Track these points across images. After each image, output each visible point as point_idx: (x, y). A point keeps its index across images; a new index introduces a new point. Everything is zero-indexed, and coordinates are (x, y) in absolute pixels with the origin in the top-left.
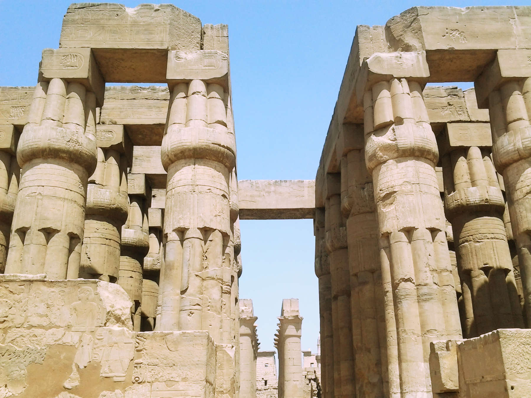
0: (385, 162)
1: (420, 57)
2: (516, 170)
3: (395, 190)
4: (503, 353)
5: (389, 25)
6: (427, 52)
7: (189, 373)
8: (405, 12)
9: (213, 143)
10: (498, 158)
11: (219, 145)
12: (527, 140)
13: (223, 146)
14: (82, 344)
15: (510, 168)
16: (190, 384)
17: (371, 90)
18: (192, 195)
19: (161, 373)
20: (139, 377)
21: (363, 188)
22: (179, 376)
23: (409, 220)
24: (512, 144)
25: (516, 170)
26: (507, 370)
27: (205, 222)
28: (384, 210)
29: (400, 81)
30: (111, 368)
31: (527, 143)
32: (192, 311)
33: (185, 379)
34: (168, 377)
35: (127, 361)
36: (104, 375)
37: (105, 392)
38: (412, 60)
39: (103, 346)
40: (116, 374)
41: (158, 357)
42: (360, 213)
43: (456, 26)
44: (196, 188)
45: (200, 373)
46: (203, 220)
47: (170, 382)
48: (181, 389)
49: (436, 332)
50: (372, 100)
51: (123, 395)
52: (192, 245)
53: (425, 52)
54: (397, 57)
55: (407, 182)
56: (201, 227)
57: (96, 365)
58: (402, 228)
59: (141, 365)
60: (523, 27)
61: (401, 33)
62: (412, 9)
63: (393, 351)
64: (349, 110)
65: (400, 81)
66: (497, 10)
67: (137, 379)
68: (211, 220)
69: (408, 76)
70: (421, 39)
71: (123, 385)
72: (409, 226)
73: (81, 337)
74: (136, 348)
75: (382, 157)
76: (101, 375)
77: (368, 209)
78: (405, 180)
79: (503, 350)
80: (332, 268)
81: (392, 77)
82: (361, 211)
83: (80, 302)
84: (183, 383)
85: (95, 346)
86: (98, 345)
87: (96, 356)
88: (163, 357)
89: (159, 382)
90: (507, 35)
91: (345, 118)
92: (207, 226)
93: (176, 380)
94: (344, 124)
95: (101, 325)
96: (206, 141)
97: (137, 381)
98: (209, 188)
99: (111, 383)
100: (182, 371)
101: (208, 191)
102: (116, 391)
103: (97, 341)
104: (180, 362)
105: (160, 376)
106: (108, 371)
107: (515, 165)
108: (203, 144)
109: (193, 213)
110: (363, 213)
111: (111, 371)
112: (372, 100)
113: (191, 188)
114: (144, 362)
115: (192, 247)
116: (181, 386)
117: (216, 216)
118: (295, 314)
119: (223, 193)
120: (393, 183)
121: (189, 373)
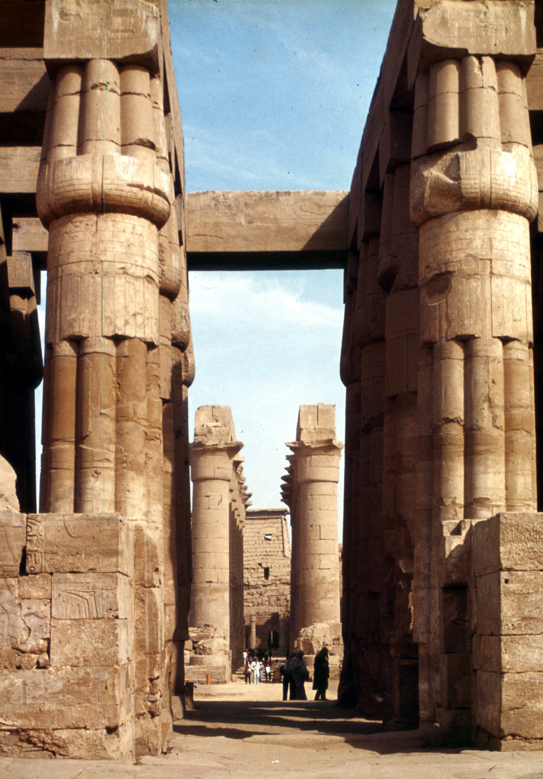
11: (141, 187)
13: (148, 189)
32: (99, 470)
46: (111, 323)
68: (126, 323)
98: (123, 265)
117: (135, 315)
118: (325, 437)
119: (146, 272)
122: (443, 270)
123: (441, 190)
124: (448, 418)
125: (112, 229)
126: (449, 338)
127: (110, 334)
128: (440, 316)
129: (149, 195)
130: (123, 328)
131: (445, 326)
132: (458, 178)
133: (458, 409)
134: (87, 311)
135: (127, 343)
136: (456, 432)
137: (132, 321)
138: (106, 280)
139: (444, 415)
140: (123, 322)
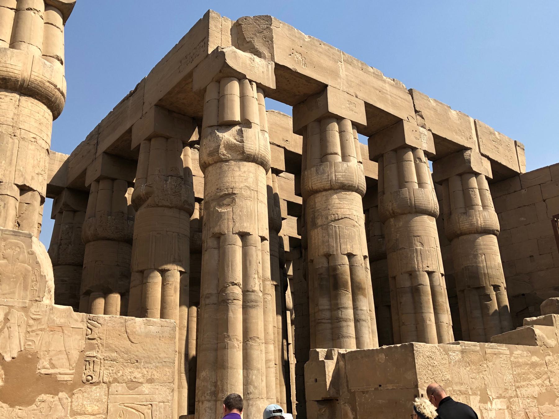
0: (227, 161)
1: (270, 66)
2: (324, 198)
3: (235, 192)
4: (416, 364)
5: (240, 22)
6: (276, 64)
7: (155, 372)
8: (260, 17)
9: (49, 82)
10: (310, 183)
11: (55, 86)
12: (340, 174)
13: (59, 90)
14: (8, 324)
15: (318, 195)
16: (157, 387)
17: (219, 82)
18: (11, 140)
19: (121, 372)
20: (93, 375)
21: (166, 181)
22: (143, 376)
23: (245, 225)
24: (327, 175)
25: (324, 198)
26: (419, 380)
27: (25, 178)
28: (219, 210)
29: (251, 84)
30: (53, 362)
31: (340, 176)
33: (150, 381)
34: (129, 377)
35: (75, 355)
36: (43, 371)
37: (43, 397)
38: (263, 68)
39: (41, 330)
40: (61, 370)
41: (117, 350)
42: (157, 206)
43: (300, 50)
44: (18, 132)
45: (168, 374)
46: (22, 175)
47: (132, 384)
48: (147, 392)
49: (257, 340)
50: (219, 93)
51: (70, 400)
52: (5, 204)
53: (274, 63)
54: (251, 58)
55: (247, 187)
56: (19, 184)
57: (30, 356)
58: (237, 232)
59: (95, 359)
60: (347, 73)
61: (252, 36)
62: (267, 16)
63: (236, 356)
64: (169, 93)
65: (251, 84)
66: (331, 49)
67: (90, 378)
68: (33, 178)
69: (258, 82)
70: (271, 49)
71: (71, 388)
72: (246, 230)
73: (6, 315)
74: (87, 335)
75: (224, 155)
76: (38, 371)
77: (168, 204)
78: (245, 184)
79: (416, 361)
80: (87, 260)
81: (244, 77)
82: (160, 204)
83: (5, 261)
84: (149, 386)
85: (29, 330)
86: (34, 329)
87: (30, 343)
88: (123, 350)
89: (118, 382)
90: (335, 74)
91: (160, 100)
92: (27, 185)
93: (140, 381)
94: (160, 106)
95: (38, 299)
96: (41, 76)
97: (88, 381)
98: (35, 136)
99: (52, 385)
100: (147, 369)
101: (33, 140)
102: (61, 395)
103: (31, 322)
104: (144, 357)
105: (119, 375)
106: (48, 366)
107: (324, 193)
108: (36, 78)
109: (11, 164)
110: (161, 206)
111: (53, 366)
112: (219, 93)
113: (11, 130)
114: (99, 355)
115: (4, 207)
116: (146, 388)
119: (48, 147)
120: (233, 185)
121: (155, 372)
122: (230, 191)
123: (230, 147)
124: (233, 282)
125: (30, 108)
126: (234, 232)
127: (20, 183)
128: (228, 219)
129: (58, 93)
130: (30, 182)
131: (231, 226)
132: (242, 141)
133: (238, 277)
134: (4, 162)
135: (30, 193)
136: (238, 291)
137: (36, 177)
138: (22, 142)
139: (231, 280)
140: (31, 178)
